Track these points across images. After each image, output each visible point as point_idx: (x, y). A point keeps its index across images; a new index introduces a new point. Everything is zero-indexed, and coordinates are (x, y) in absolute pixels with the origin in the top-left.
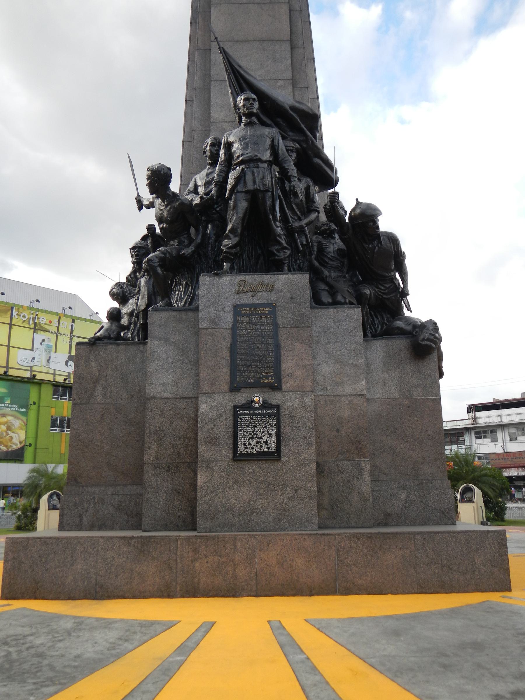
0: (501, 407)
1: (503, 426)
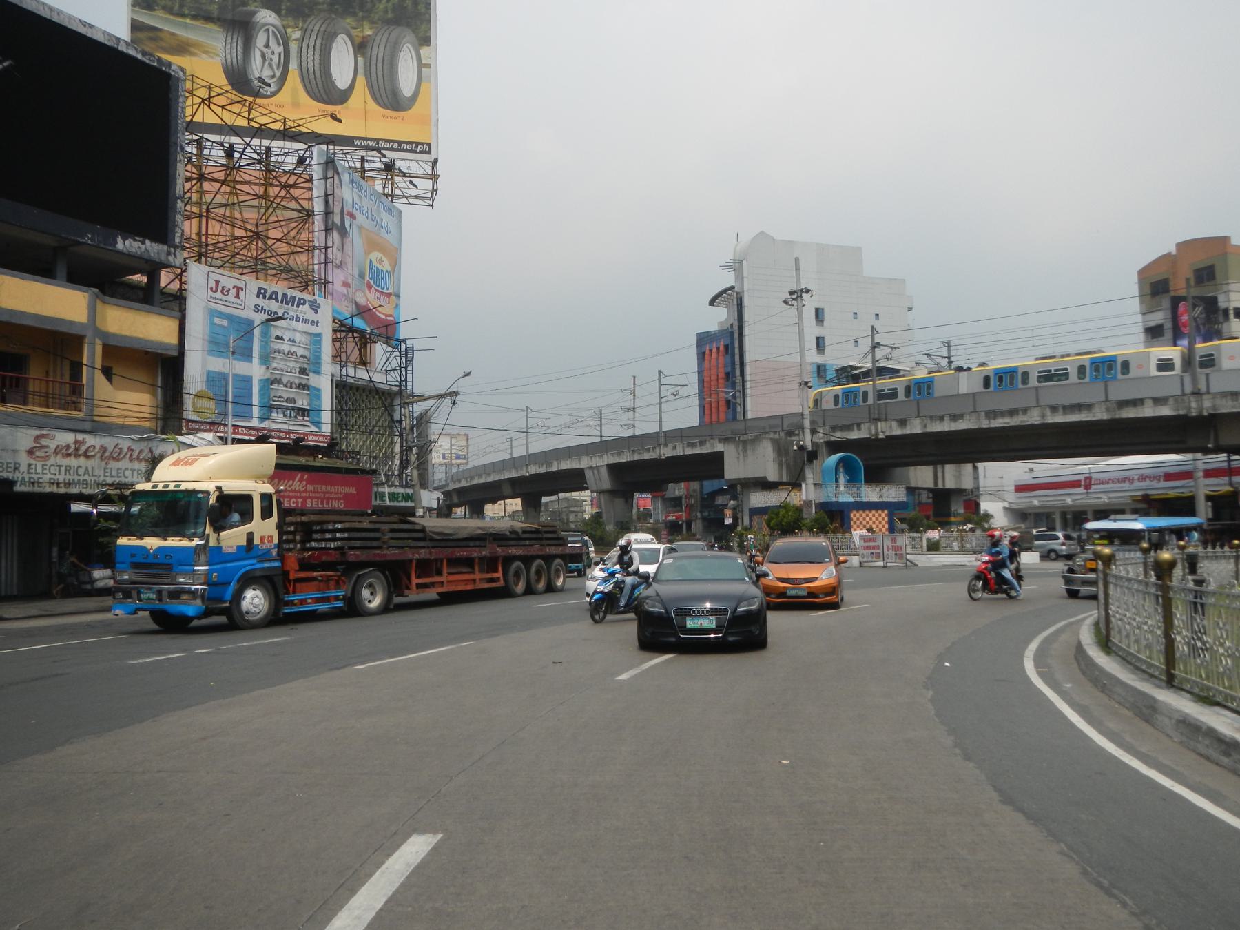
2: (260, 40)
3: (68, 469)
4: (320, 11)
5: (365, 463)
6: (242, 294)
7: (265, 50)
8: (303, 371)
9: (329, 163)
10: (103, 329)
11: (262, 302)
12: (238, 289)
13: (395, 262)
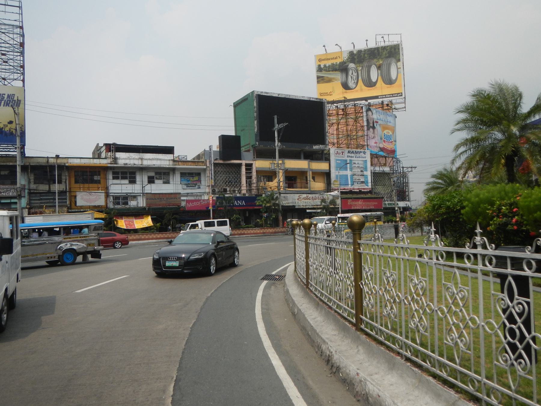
0: (141, 151)
1: (143, 169)
2: (350, 73)
3: (306, 202)
4: (366, 59)
5: (380, 196)
6: (344, 154)
7: (352, 75)
8: (362, 171)
9: (369, 110)
10: (312, 168)
11: (349, 154)
12: (343, 152)
13: (394, 131)
